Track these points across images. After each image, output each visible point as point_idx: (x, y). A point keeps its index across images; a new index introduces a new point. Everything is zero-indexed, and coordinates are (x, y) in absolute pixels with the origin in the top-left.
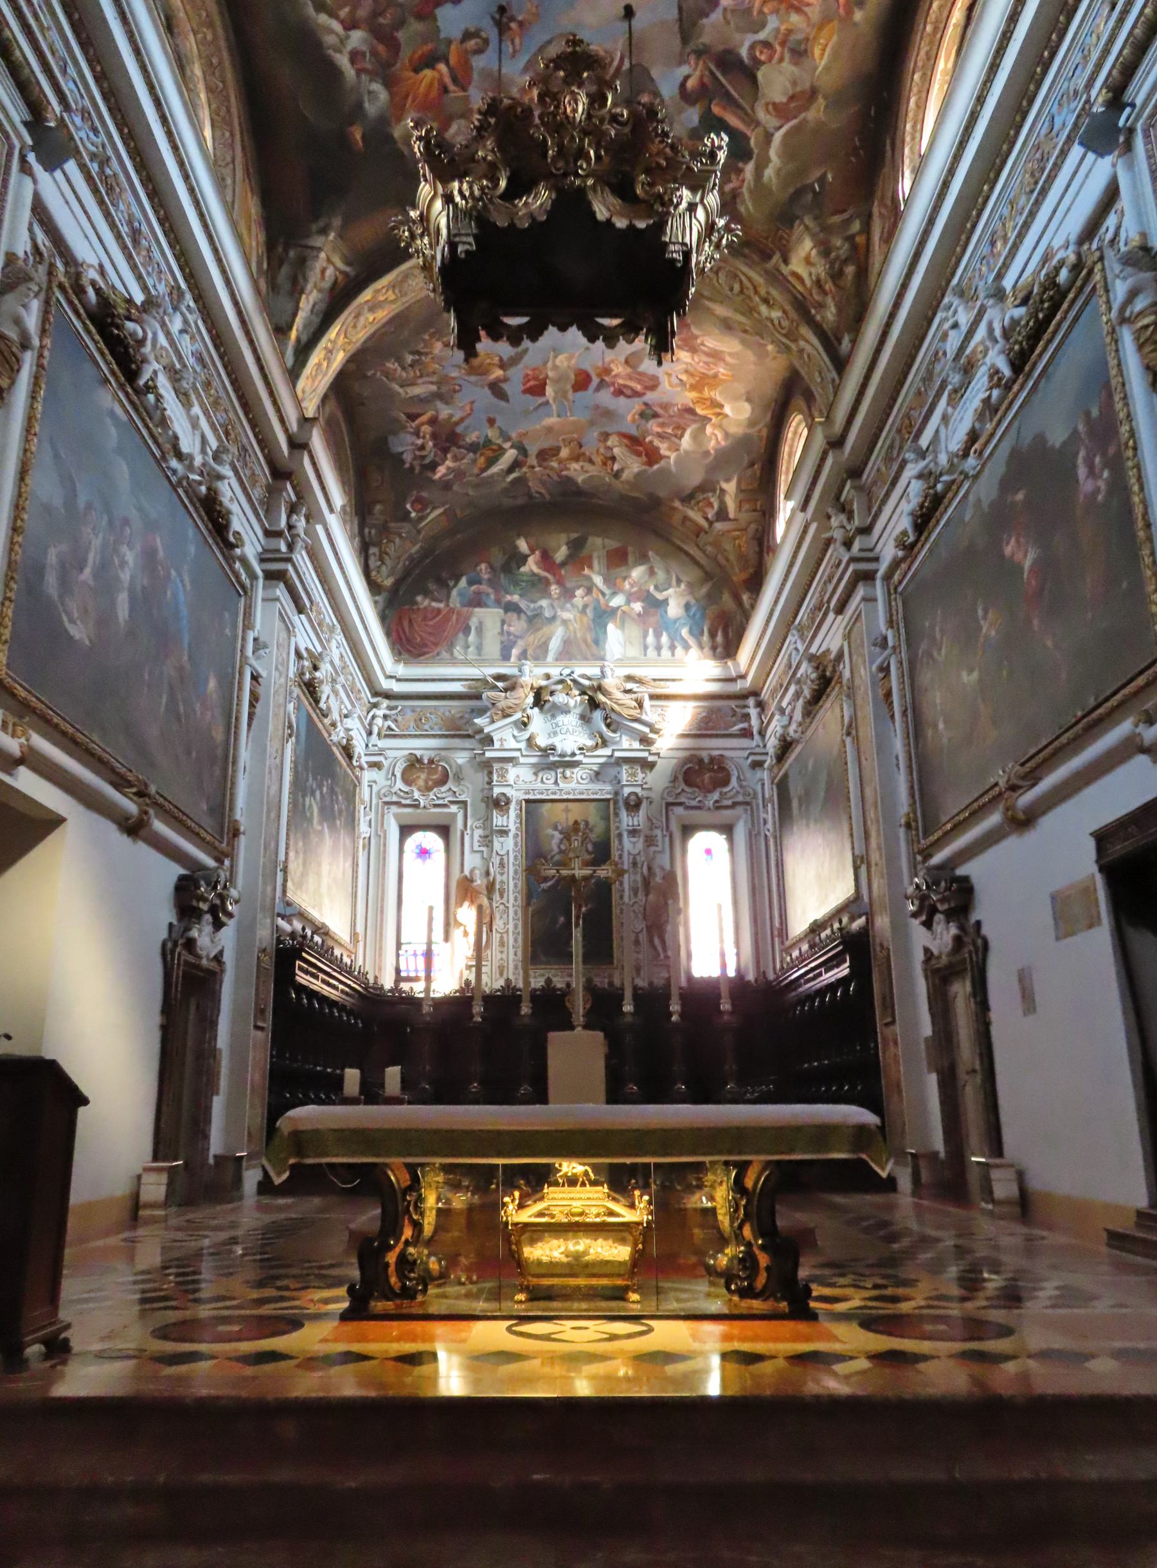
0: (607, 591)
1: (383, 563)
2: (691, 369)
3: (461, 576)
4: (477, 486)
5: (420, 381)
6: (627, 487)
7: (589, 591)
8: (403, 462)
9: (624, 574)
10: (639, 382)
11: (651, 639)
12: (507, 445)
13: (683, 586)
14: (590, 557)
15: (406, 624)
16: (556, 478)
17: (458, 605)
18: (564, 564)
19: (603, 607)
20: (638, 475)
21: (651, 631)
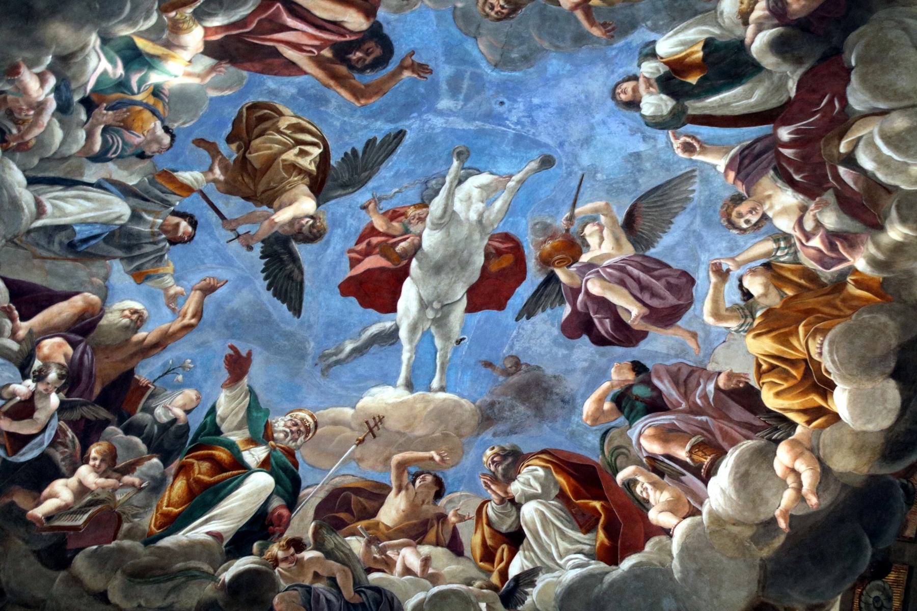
2: (783, 256)
5: (93, 173)
10: (641, 290)
16: (349, 593)
20: (571, 592)
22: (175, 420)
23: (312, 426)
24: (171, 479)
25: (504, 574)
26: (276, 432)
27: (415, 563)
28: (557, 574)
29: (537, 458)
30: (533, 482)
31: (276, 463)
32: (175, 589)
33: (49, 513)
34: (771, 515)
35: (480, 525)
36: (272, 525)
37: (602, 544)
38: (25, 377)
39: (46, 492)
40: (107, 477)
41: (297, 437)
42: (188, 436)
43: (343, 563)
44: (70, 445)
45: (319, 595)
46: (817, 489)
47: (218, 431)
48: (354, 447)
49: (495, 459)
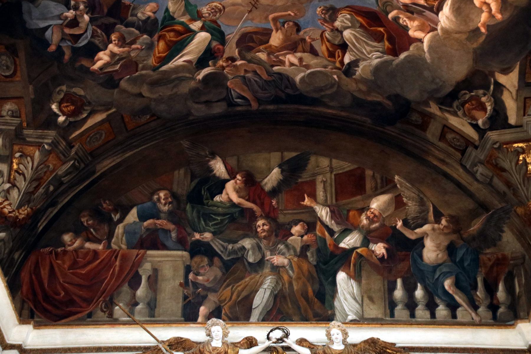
0: (336, 228)
1: (14, 186)
3: (132, 208)
4: (154, 84)
6: (363, 88)
7: (310, 227)
8: (47, 44)
9: (360, 206)
11: (399, 293)
12: (196, 25)
13: (444, 222)
14: (312, 184)
15: (44, 273)
16: (265, 76)
17: (124, 246)
18: (275, 192)
19: (331, 248)
20: (377, 69)
21: (399, 282)
22: (149, 18)
23: (222, 8)
24: (156, 43)
25: (342, 62)
26: (203, 14)
27: (295, 61)
28: (368, 61)
29: (344, 10)
30: (345, 21)
31: (208, 27)
32: (175, 86)
33: (100, 67)
34: (476, 27)
35: (324, 42)
36: (216, 53)
37: (388, 47)
38: (69, 9)
39: (96, 58)
40: (124, 47)
41: (215, 14)
42: (158, 23)
43: (258, 64)
44: (101, 36)
45: (250, 80)
46: (501, 10)
47: (173, 18)
48: (247, 14)
49: (323, 12)
